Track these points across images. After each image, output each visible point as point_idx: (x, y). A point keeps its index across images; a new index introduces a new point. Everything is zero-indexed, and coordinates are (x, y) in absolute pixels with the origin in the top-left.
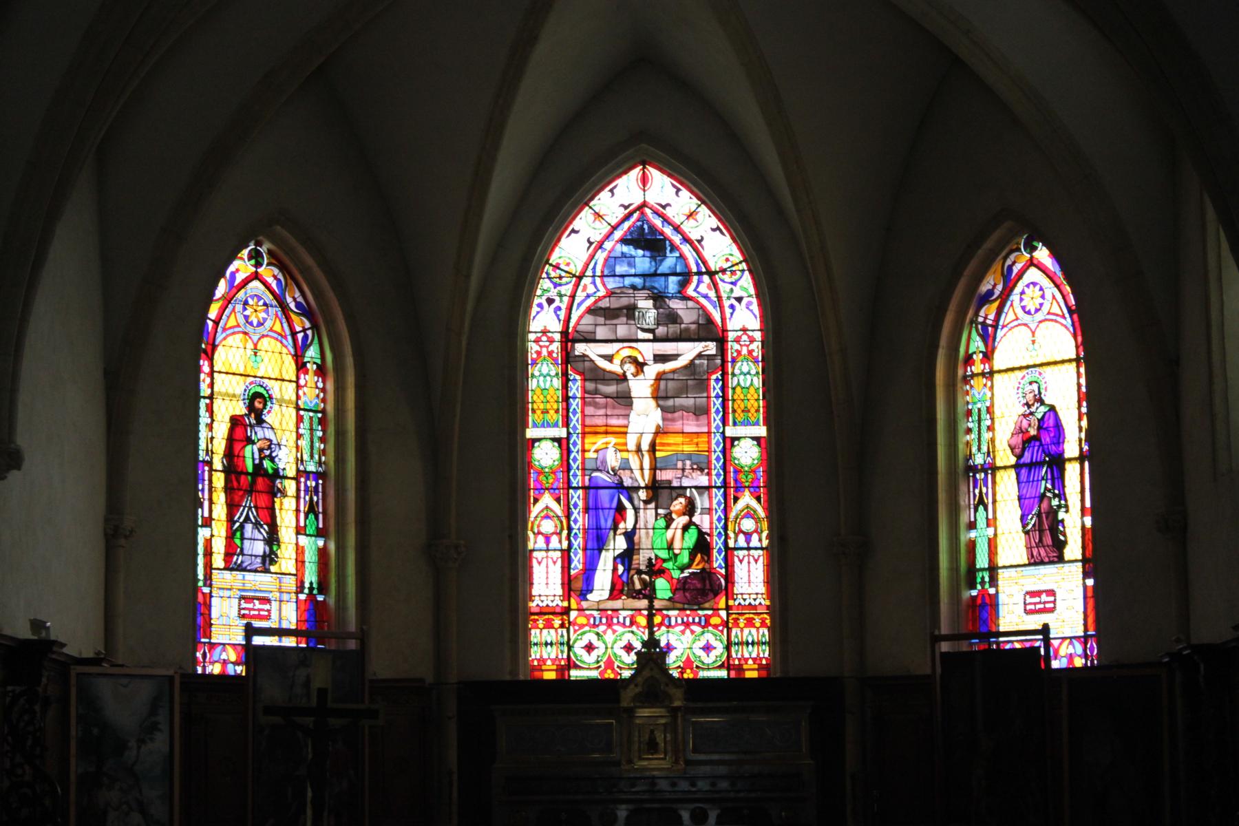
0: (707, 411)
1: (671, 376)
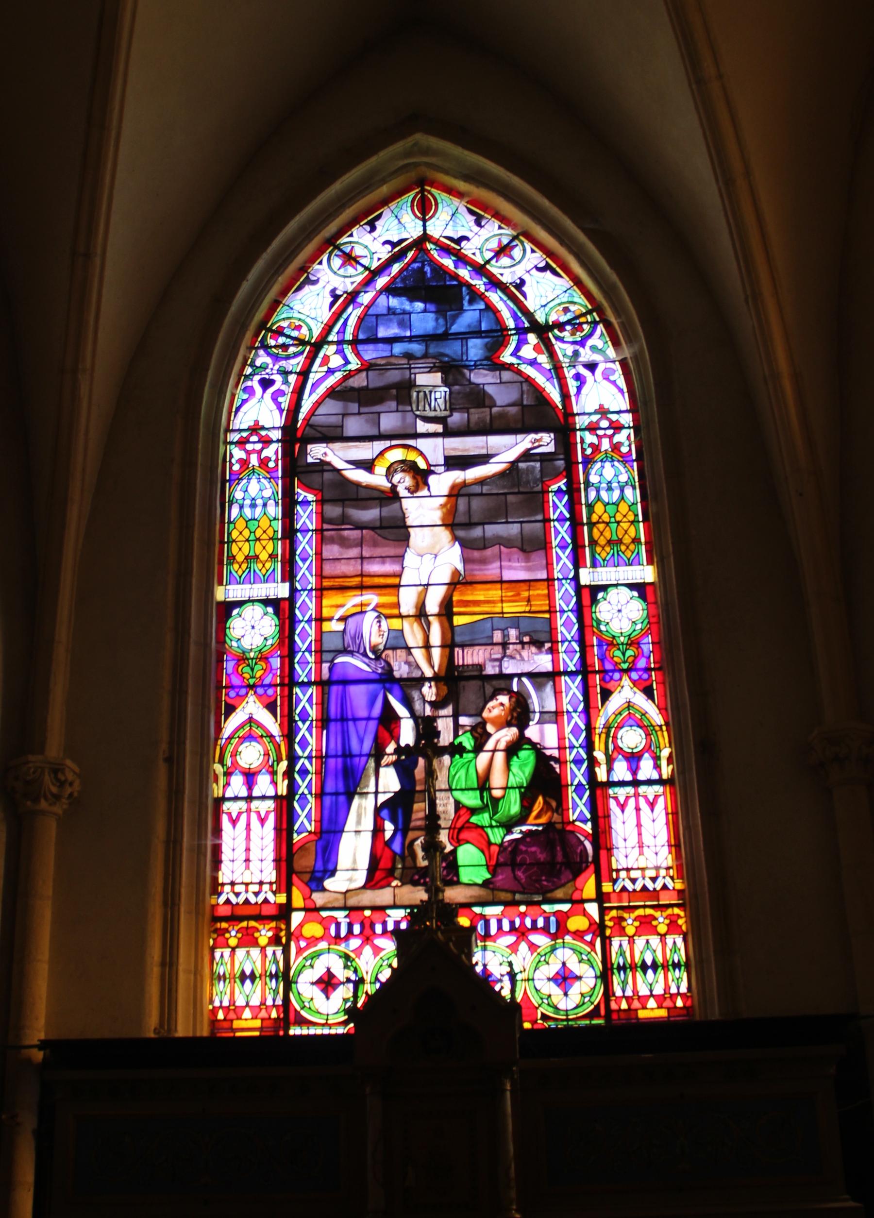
0: (546, 546)
1: (477, 489)
